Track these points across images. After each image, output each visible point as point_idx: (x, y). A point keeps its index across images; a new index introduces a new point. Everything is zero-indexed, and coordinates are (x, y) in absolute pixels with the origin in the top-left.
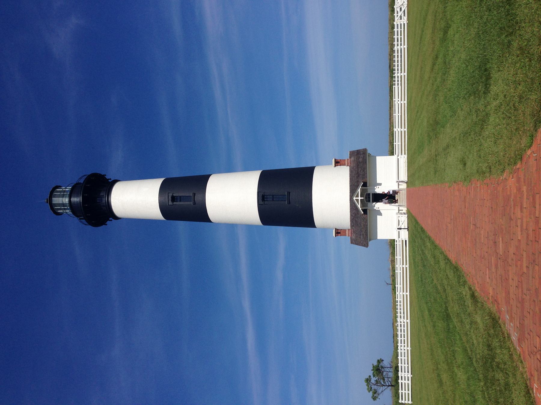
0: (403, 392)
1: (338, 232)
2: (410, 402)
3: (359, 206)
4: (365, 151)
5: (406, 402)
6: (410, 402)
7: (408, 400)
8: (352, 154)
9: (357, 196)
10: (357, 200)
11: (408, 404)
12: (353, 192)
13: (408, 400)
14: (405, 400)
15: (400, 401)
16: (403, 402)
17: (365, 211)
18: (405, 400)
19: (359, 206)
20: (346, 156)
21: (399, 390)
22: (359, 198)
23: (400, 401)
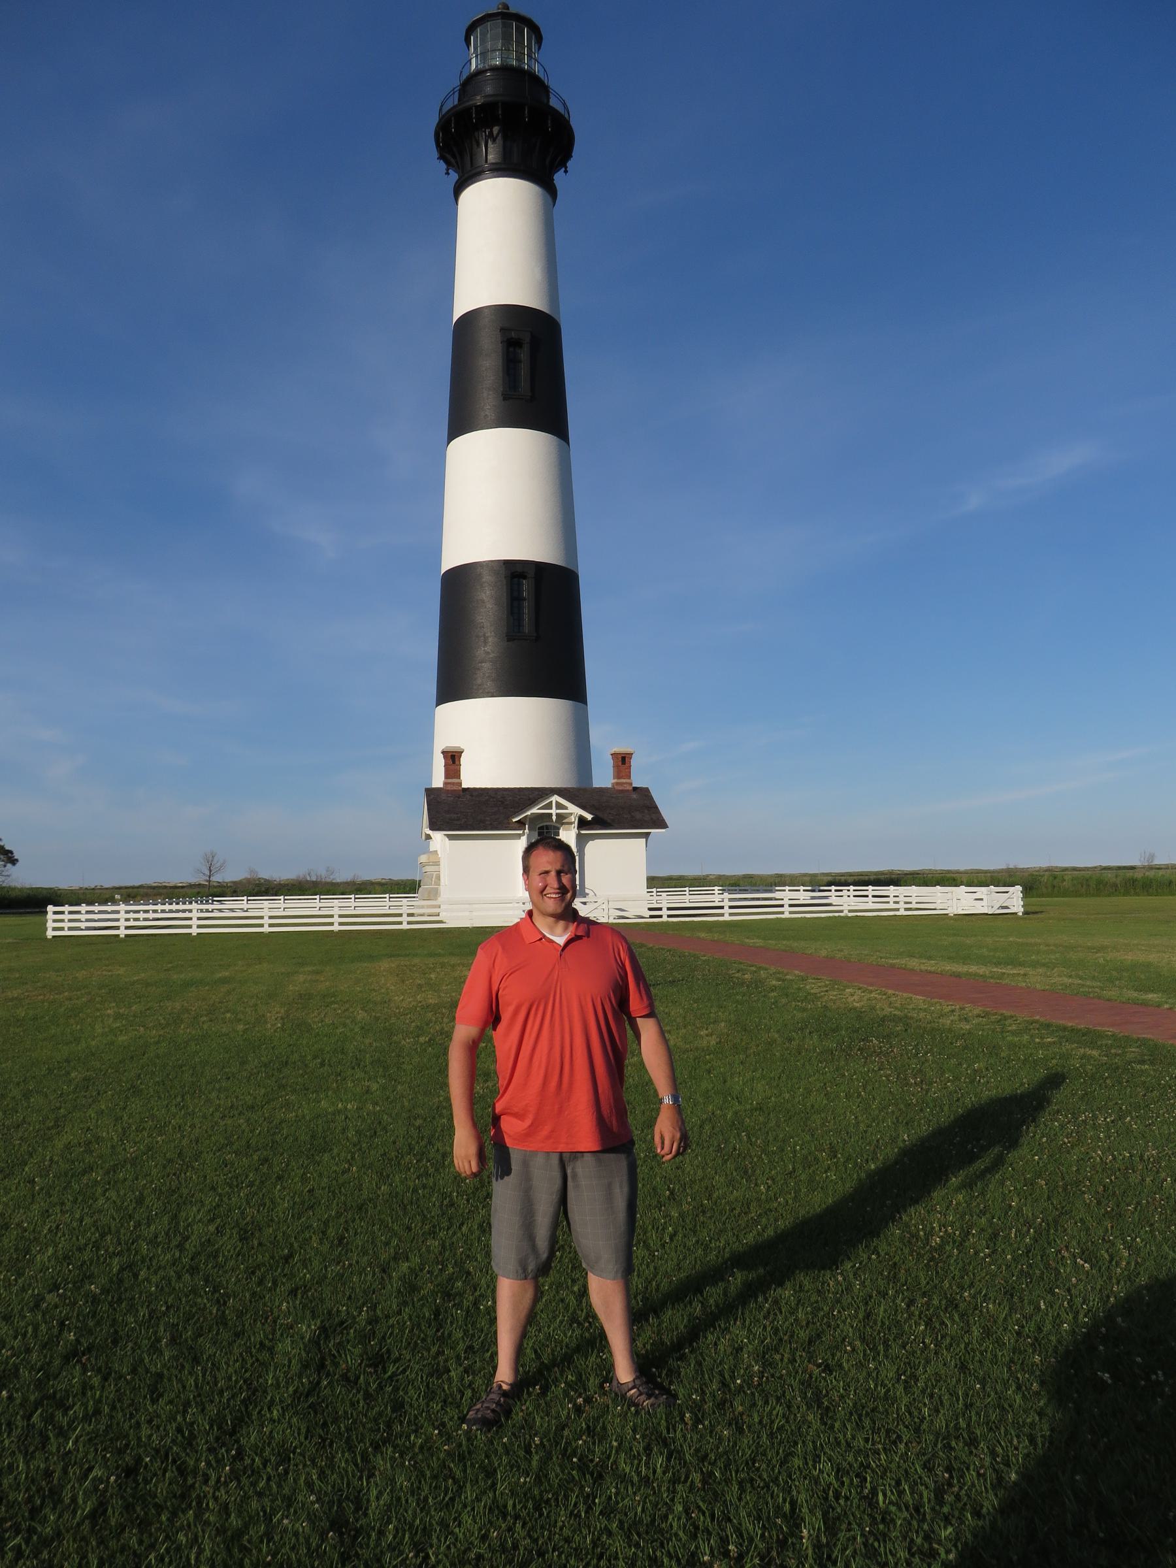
1: (453, 758)
2: (50, 934)
3: (535, 810)
4: (661, 823)
5: (50, 925)
6: (50, 934)
7: (55, 929)
8: (644, 793)
10: (549, 806)
11: (46, 929)
13: (55, 929)
14: (55, 921)
15: (50, 908)
16: (50, 916)
18: (55, 921)
19: (535, 810)
20: (637, 781)
21: (71, 905)
22: (554, 811)
23: (50, 908)
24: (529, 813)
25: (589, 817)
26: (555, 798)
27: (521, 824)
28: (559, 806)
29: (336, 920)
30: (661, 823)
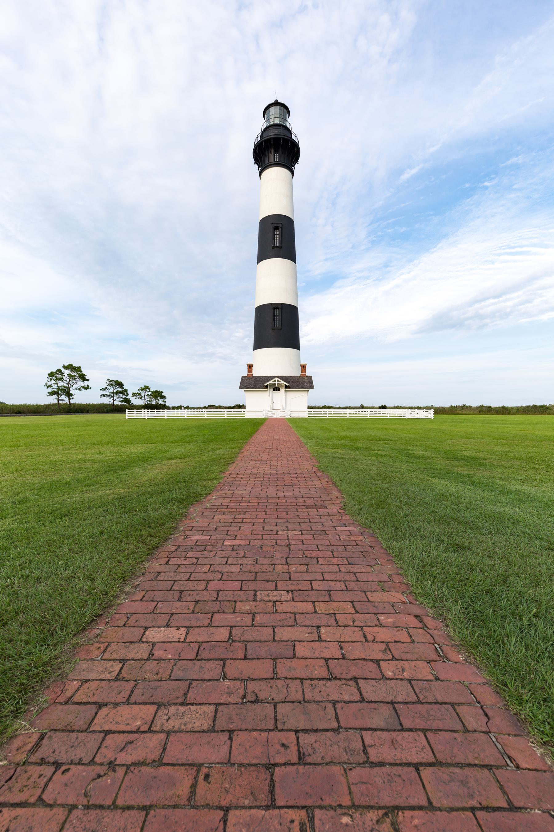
0: (135, 413)
2: (127, 417)
3: (270, 382)
4: (312, 387)
8: (310, 378)
9: (278, 381)
10: (275, 381)
12: (282, 378)
15: (127, 410)
16: (127, 412)
17: (267, 387)
20: (308, 373)
22: (276, 383)
23: (127, 410)
24: (268, 383)
25: (288, 385)
26: (277, 379)
27: (267, 387)
28: (278, 381)
29: (206, 415)
30: (312, 387)
